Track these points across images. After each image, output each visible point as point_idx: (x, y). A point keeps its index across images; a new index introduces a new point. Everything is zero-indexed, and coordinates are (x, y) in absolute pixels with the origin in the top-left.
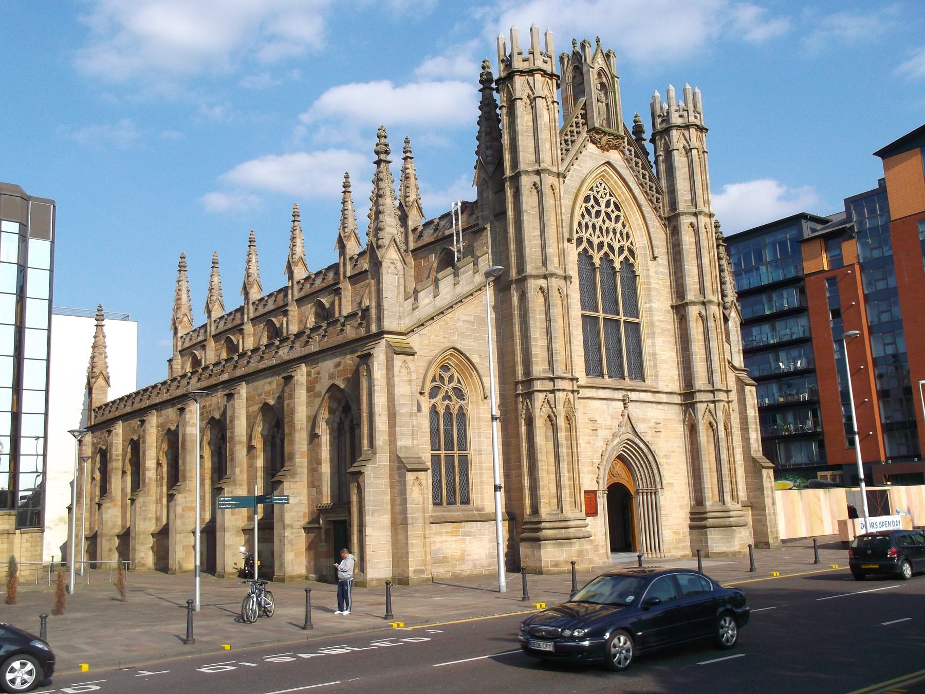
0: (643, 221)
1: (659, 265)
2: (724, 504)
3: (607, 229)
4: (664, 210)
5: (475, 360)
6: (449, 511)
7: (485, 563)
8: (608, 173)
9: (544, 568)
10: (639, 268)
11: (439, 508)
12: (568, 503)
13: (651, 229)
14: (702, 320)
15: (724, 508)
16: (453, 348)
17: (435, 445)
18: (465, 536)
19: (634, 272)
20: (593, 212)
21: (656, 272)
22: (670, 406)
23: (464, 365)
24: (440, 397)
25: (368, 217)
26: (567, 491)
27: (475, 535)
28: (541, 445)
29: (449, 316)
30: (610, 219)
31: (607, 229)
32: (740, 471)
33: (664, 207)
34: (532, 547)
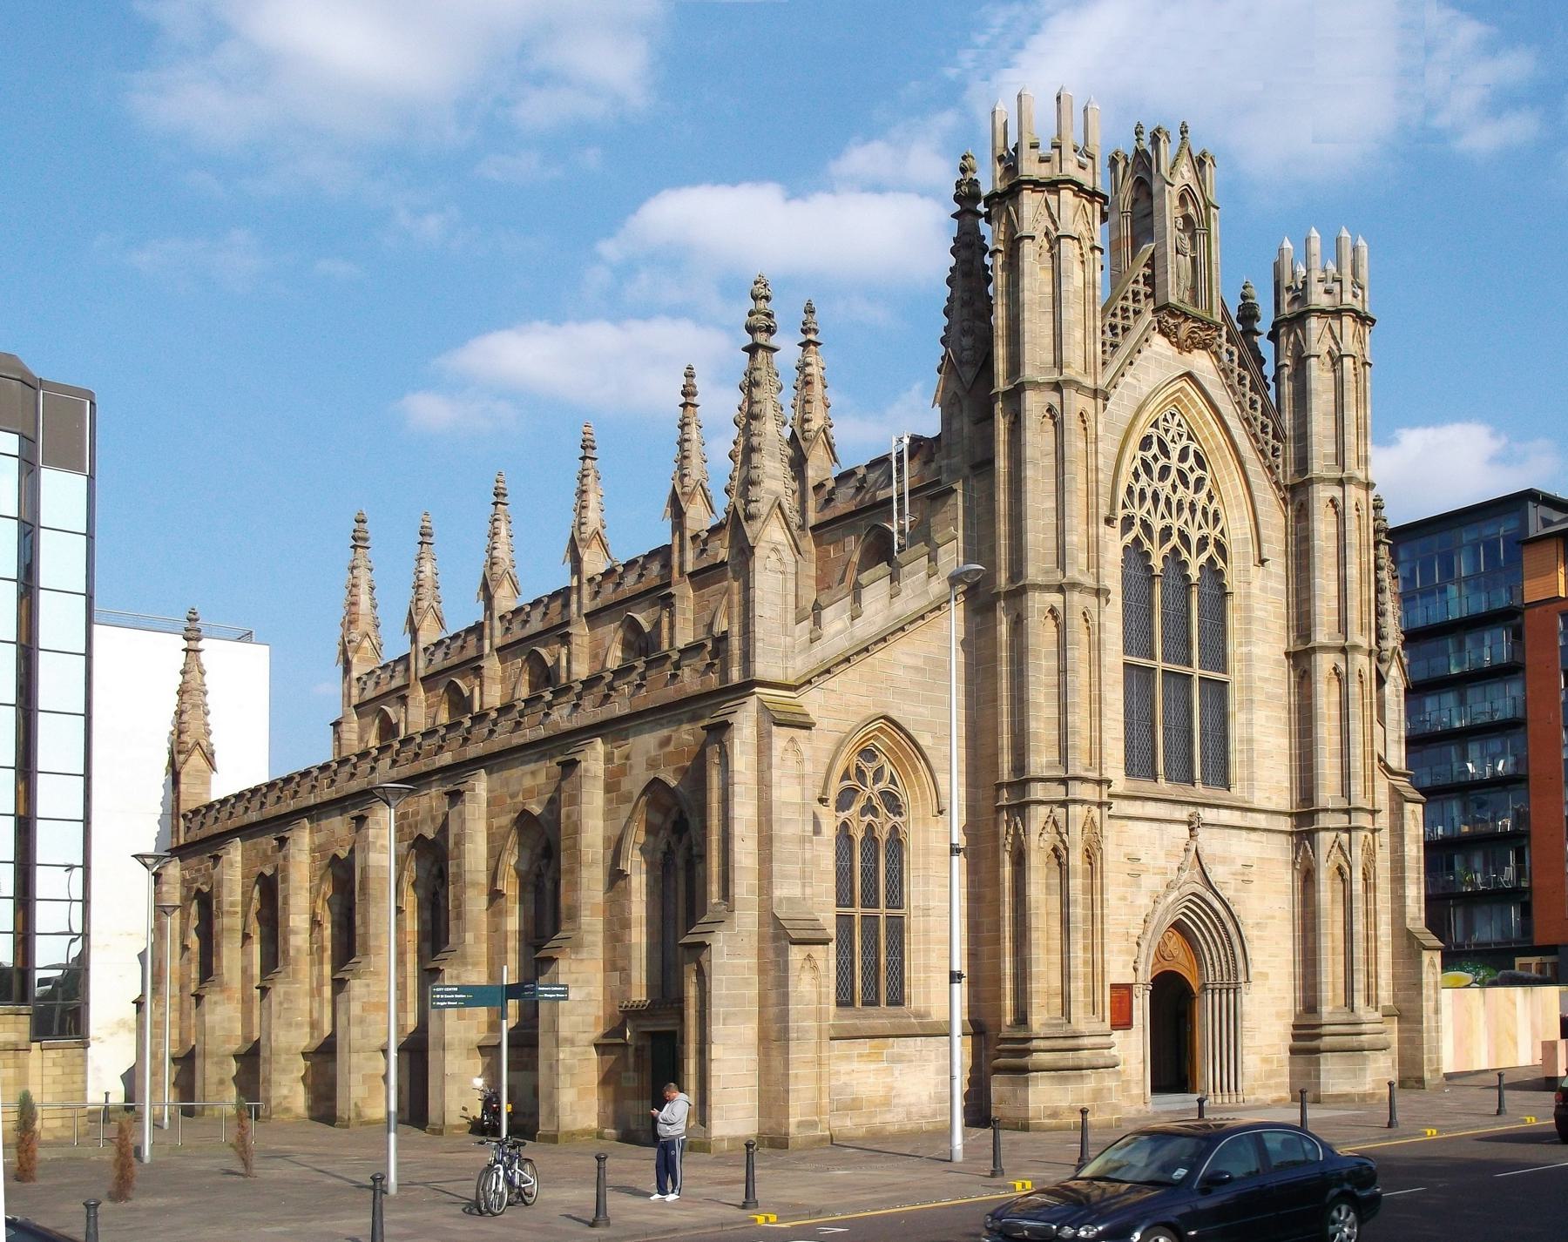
0: (1246, 492)
1: (1269, 574)
2: (1352, 1011)
3: (1180, 503)
4: (1285, 472)
5: (924, 740)
6: (867, 1017)
7: (927, 1111)
9: (1032, 1119)
10: (1232, 580)
11: (848, 1011)
12: (1081, 1005)
13: (1258, 506)
14: (1339, 680)
15: (1352, 1018)
16: (885, 718)
17: (844, 896)
18: (893, 1062)
19: (1223, 586)
20: (1156, 468)
21: (1263, 589)
23: (903, 750)
24: (856, 808)
25: (730, 457)
26: (1081, 984)
27: (912, 1061)
28: (1037, 902)
29: (880, 656)
30: (1186, 484)
31: (1180, 503)
32: (1385, 954)
33: (1285, 466)
34: (1014, 1083)
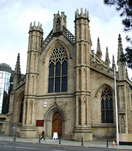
8: (59, 42)
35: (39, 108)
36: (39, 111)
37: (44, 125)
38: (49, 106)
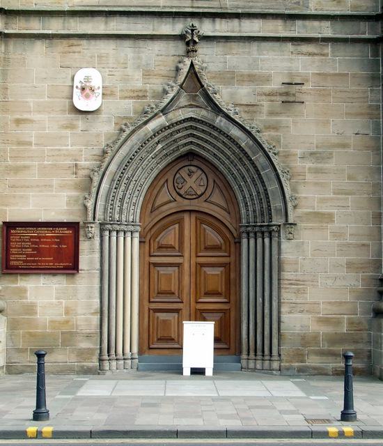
22: (341, 47)
35: (18, 122)
36: (19, 143)
37: (83, 264)
38: (128, 107)
